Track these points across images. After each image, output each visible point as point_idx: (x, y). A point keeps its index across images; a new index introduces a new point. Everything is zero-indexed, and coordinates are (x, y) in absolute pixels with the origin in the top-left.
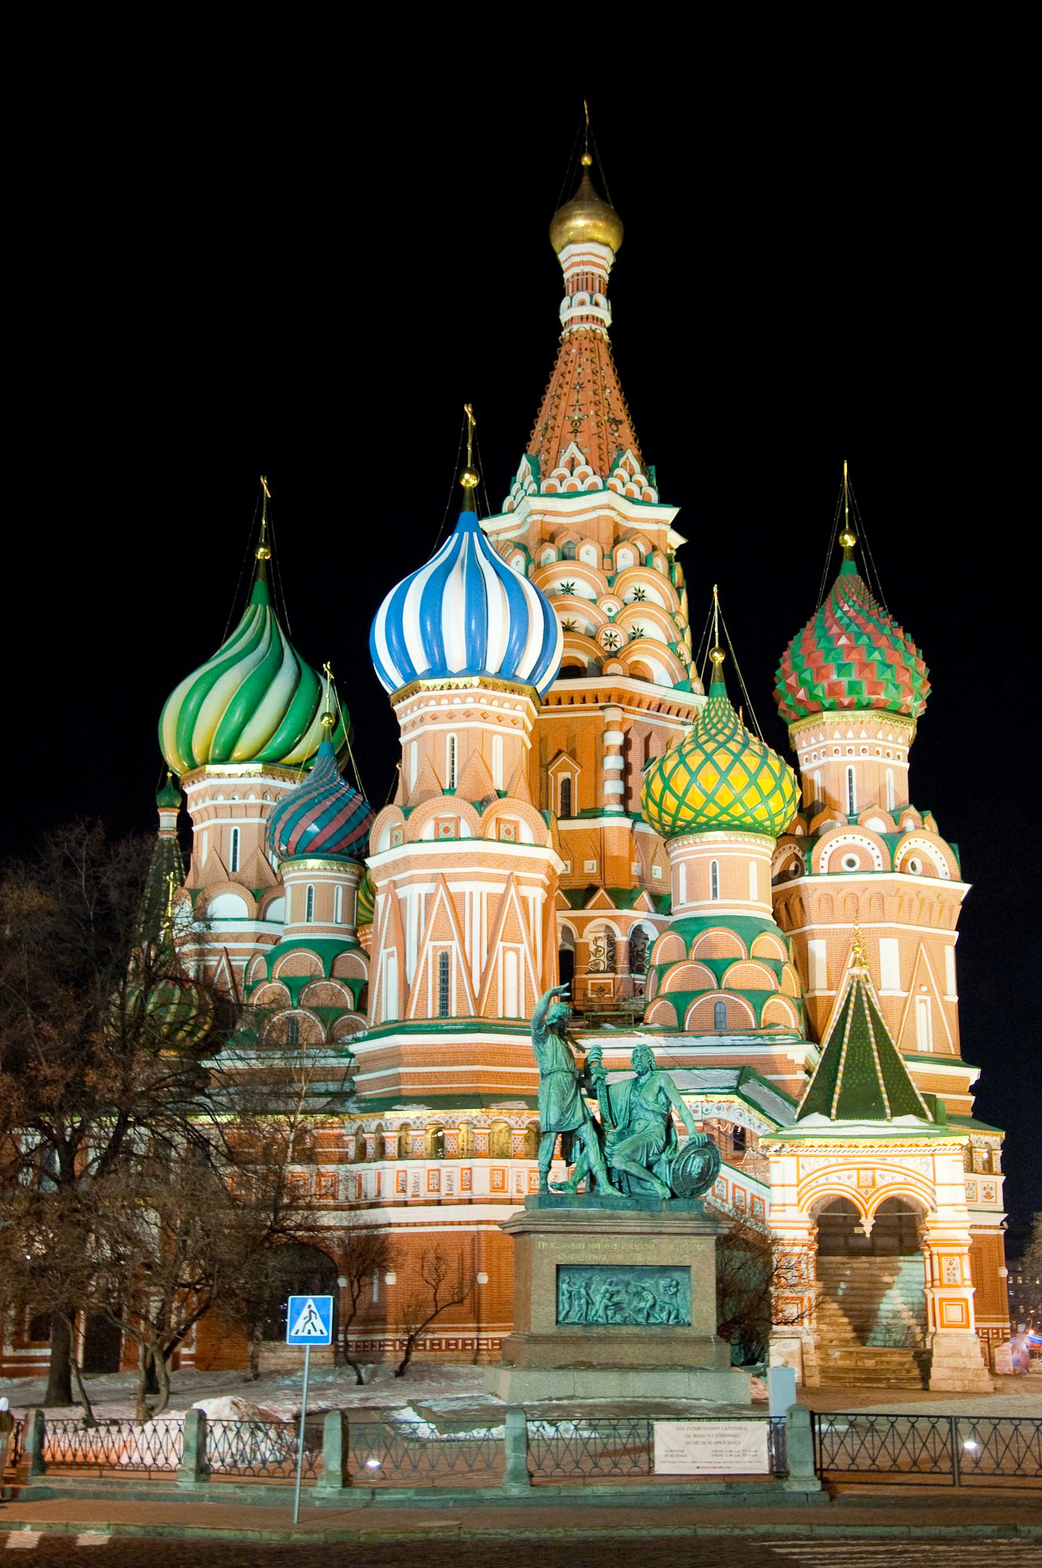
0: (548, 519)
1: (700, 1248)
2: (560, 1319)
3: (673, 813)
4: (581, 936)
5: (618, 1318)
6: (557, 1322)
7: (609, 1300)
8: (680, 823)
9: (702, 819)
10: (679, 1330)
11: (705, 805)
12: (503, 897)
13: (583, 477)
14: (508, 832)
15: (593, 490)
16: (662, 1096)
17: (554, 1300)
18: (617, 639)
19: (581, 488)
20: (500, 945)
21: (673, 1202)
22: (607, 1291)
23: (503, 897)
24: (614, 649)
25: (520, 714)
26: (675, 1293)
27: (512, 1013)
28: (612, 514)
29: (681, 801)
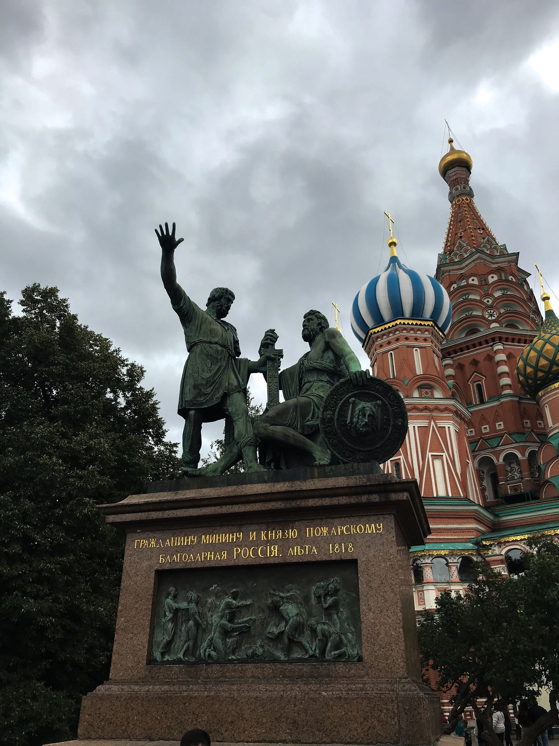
0: (451, 273)
1: (371, 528)
2: (157, 655)
3: (533, 377)
4: (498, 461)
5: (245, 651)
6: (151, 661)
7: (231, 621)
8: (539, 382)
9: (551, 376)
10: (340, 668)
11: (551, 367)
12: (427, 428)
13: (466, 251)
14: (427, 393)
15: (472, 254)
16: (330, 355)
17: (147, 623)
18: (495, 313)
19: (465, 256)
20: (429, 454)
21: (328, 469)
22: (228, 606)
23: (427, 428)
24: (493, 318)
25: (427, 335)
26: (335, 606)
27: (442, 493)
28: (482, 261)
29: (536, 368)
